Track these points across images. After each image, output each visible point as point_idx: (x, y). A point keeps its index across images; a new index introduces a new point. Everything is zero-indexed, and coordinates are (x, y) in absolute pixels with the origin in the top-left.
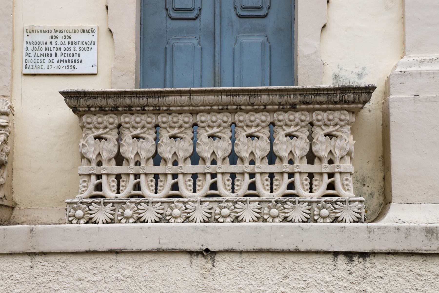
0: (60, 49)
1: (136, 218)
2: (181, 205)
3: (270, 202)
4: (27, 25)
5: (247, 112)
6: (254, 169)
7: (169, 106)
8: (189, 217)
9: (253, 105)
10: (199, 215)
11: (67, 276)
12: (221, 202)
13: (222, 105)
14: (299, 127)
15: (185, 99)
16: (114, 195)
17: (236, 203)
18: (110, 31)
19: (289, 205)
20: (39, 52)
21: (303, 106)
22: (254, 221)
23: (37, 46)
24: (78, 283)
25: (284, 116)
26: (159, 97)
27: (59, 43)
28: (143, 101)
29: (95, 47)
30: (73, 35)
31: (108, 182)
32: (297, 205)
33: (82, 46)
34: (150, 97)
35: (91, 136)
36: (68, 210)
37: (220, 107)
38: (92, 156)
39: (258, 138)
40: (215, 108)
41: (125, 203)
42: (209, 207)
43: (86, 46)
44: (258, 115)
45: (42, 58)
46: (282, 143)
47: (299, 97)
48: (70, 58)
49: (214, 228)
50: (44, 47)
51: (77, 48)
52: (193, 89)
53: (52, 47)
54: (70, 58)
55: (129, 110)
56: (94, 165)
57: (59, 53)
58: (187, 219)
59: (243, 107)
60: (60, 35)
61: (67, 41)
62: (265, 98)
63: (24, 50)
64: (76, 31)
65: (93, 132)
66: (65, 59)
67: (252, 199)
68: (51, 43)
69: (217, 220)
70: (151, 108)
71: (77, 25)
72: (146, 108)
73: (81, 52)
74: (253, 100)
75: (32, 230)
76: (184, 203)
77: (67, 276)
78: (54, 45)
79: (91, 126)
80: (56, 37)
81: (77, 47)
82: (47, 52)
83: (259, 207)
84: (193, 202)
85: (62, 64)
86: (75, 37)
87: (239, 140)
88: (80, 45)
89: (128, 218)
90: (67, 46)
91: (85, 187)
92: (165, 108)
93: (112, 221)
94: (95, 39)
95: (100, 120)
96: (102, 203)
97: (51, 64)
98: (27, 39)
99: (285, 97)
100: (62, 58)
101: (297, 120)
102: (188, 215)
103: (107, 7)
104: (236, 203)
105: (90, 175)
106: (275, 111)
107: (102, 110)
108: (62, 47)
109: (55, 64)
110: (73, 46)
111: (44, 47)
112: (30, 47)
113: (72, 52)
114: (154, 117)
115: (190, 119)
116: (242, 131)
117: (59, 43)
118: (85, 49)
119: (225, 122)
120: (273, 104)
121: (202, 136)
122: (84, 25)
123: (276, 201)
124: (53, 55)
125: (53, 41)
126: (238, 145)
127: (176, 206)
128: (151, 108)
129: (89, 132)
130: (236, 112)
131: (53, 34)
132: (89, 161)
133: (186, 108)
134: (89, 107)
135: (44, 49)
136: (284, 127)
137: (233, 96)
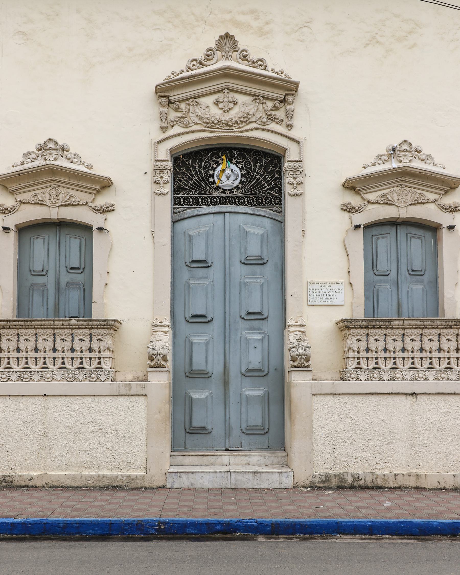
0: (326, 292)
1: (379, 378)
2: (400, 372)
3: (441, 371)
4: (309, 280)
5: (428, 329)
6: (432, 355)
7: (393, 326)
8: (404, 378)
9: (432, 326)
10: (408, 377)
11: (350, 404)
12: (418, 371)
13: (417, 326)
14: (452, 336)
15: (401, 323)
16: (366, 367)
17: (425, 371)
18: (350, 283)
19: (450, 373)
20: (315, 294)
21: (455, 327)
22: (434, 380)
23: (314, 291)
24: (355, 408)
25: (445, 331)
26: (388, 322)
27: (325, 289)
28: (381, 323)
29: (343, 291)
30: (332, 285)
31: (363, 361)
32: (453, 372)
33: (337, 291)
34: (384, 321)
35: (355, 339)
36: (347, 374)
37: (417, 327)
38: (356, 349)
39: (433, 341)
40: (414, 327)
41: (374, 371)
42: (413, 373)
43: (339, 291)
44: (434, 330)
45: (317, 297)
46: (445, 343)
47: (454, 323)
48: (331, 297)
49: (417, 383)
50: (318, 291)
51: (334, 292)
52: (406, 318)
53: (322, 291)
54: (331, 297)
55: (374, 327)
56: (356, 353)
57: (325, 295)
58: (403, 379)
59: (427, 327)
60: (326, 285)
61: (329, 288)
62: (438, 323)
63: (308, 293)
64: (333, 283)
65: (355, 337)
66: (328, 297)
67: (432, 369)
68: (321, 289)
69: (417, 380)
70: (384, 327)
71: (334, 280)
72: (382, 327)
73: (336, 294)
74: (432, 324)
75: (333, 383)
76: (401, 371)
77: (350, 404)
78: (323, 290)
79: (354, 334)
80: (324, 286)
81: (334, 291)
82: (319, 294)
83: (436, 373)
84: (405, 371)
85: (327, 300)
86: (333, 287)
87: (425, 342)
88: (335, 290)
89: (375, 378)
90: (329, 291)
91: (352, 363)
92: (391, 327)
93: (368, 379)
94: (343, 287)
95: (359, 332)
96: (363, 371)
97: (322, 300)
98: (309, 287)
99: (448, 323)
100: (327, 297)
101: (452, 333)
102: (404, 377)
103: (349, 272)
104: (425, 371)
105: (354, 358)
106: (441, 328)
107: (361, 327)
108: (327, 291)
109: (324, 300)
110: (332, 291)
111: (318, 291)
112: (311, 291)
113: (332, 294)
114: (384, 330)
115: (402, 332)
116: (426, 337)
117: (325, 289)
118: (338, 292)
119: (418, 333)
120: (441, 325)
121: (407, 340)
122: (337, 280)
123: (444, 371)
124: (323, 295)
125: (322, 288)
126: (424, 344)
127: (397, 373)
128: (384, 327)
129: (353, 337)
130: (423, 329)
131: (322, 285)
132: (354, 351)
133: (401, 327)
134: (355, 326)
135: (318, 292)
136: (445, 336)
137: (424, 322)
